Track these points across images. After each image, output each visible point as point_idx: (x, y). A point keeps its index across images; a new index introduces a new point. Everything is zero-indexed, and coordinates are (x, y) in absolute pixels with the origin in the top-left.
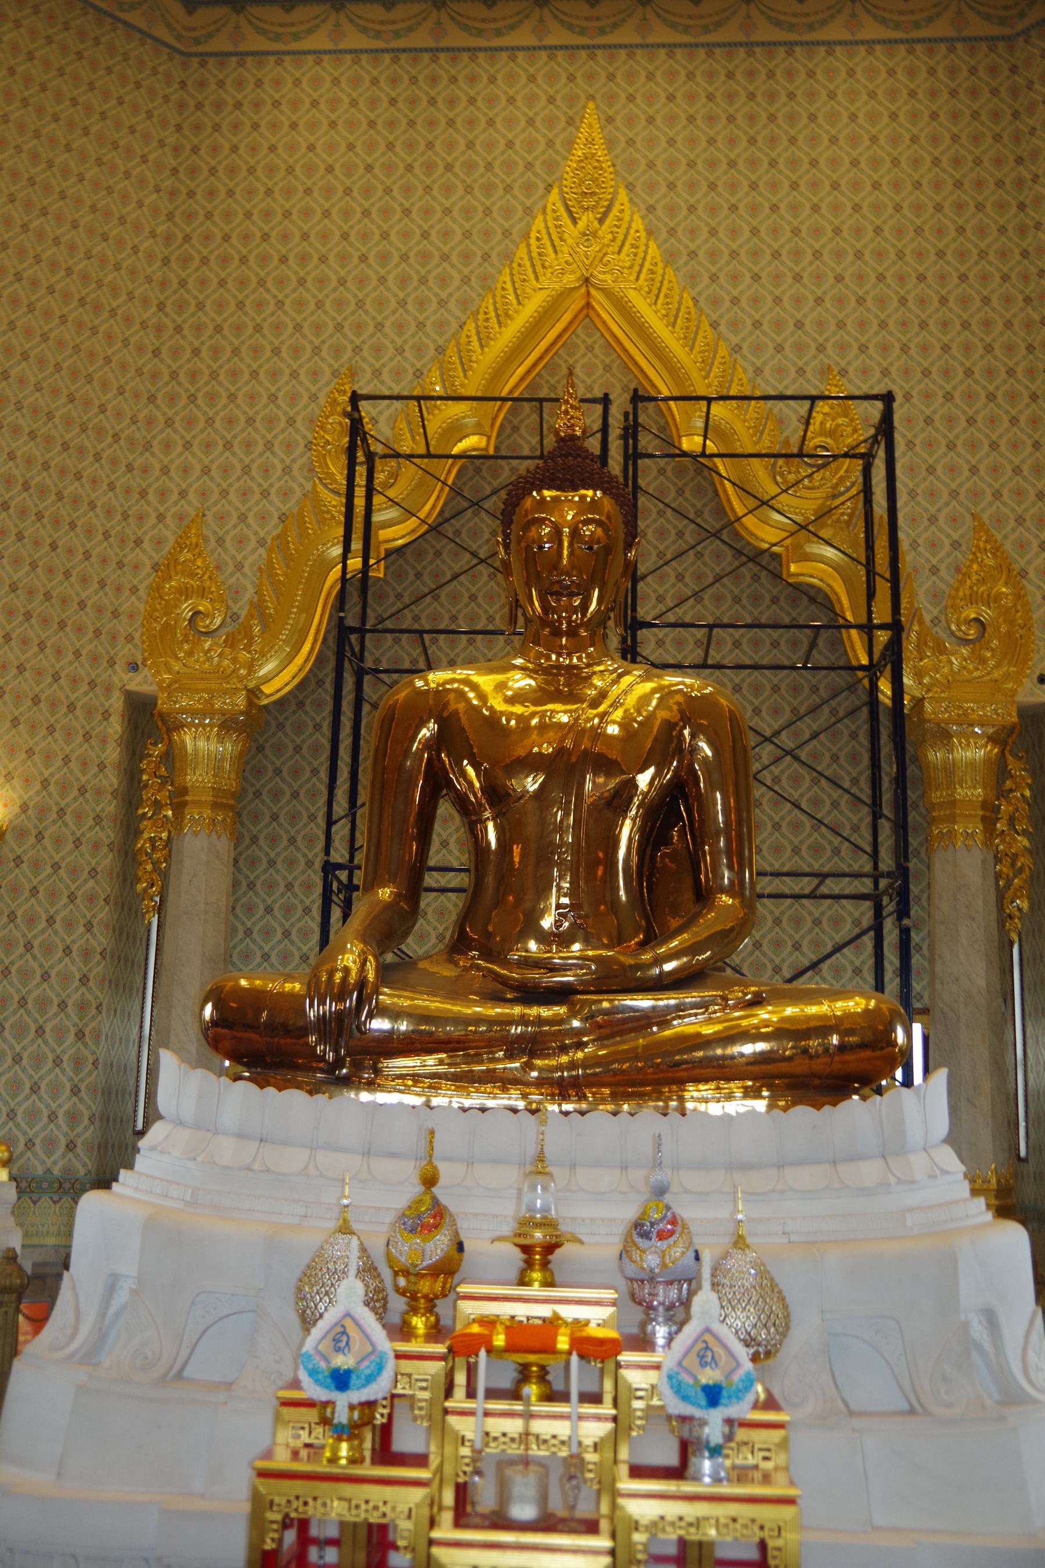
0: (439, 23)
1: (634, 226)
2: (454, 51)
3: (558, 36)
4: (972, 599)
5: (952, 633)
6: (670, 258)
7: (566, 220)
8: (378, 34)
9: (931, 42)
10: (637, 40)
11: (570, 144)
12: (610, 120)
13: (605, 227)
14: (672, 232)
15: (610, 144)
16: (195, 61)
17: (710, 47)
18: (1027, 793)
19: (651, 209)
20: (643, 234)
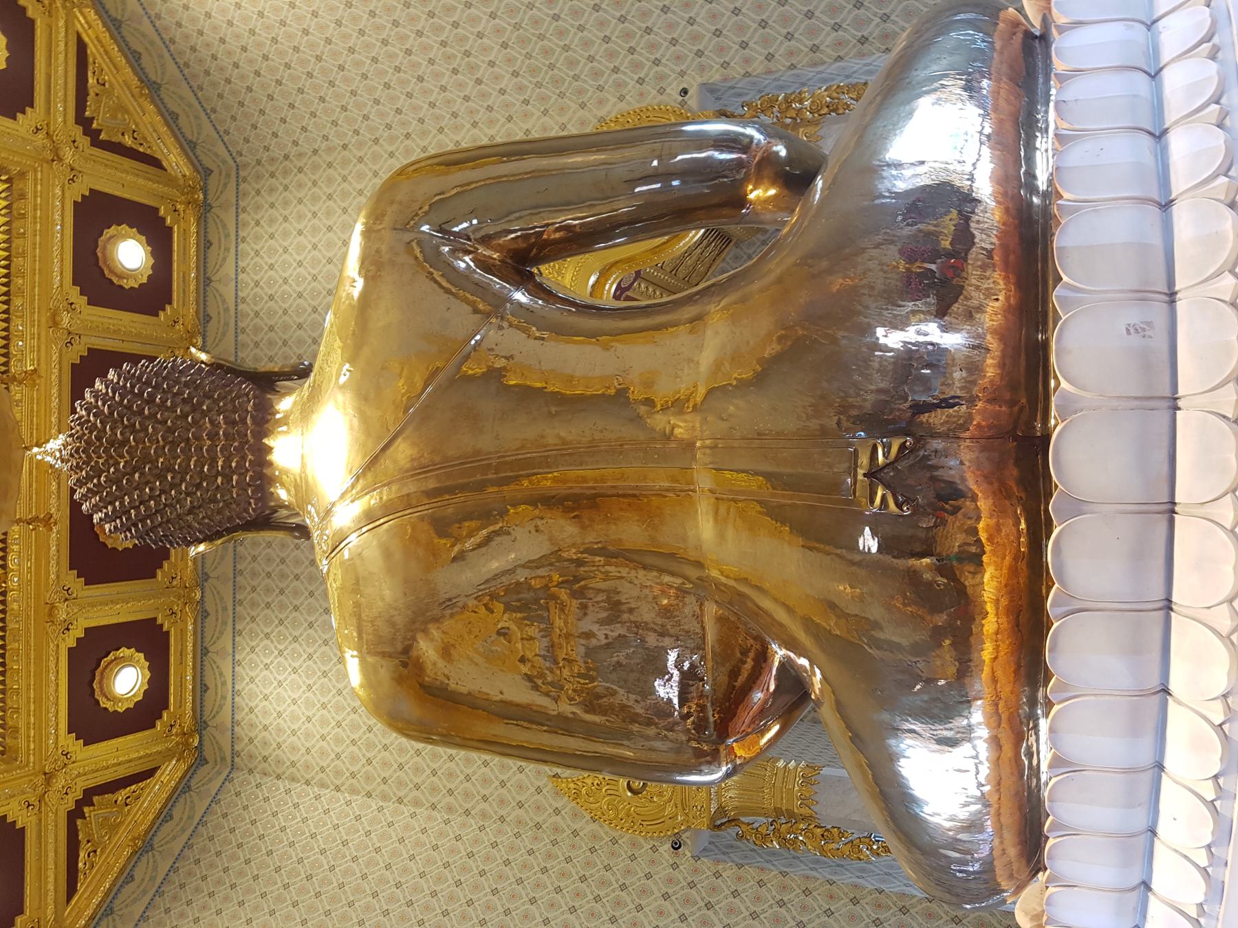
16: (236, 760)
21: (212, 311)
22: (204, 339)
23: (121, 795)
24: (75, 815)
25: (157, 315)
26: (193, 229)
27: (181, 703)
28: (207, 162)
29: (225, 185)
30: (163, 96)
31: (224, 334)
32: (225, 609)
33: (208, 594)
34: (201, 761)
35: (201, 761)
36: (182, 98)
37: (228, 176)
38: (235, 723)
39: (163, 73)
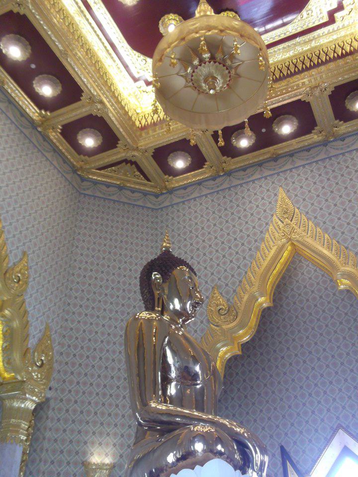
0: (230, 180)
2: (235, 186)
3: (267, 173)
6: (317, 225)
7: (280, 223)
10: (292, 167)
11: (277, 201)
12: (288, 191)
13: (293, 221)
14: (316, 218)
15: (290, 198)
17: (317, 162)
19: (307, 213)
21: (347, 140)
22: (333, 141)
23: (138, 173)
24: (126, 161)
25: (336, 119)
27: (177, 182)
31: (337, 149)
32: (218, 187)
33: (223, 178)
34: (157, 196)
35: (157, 196)
38: (172, 206)
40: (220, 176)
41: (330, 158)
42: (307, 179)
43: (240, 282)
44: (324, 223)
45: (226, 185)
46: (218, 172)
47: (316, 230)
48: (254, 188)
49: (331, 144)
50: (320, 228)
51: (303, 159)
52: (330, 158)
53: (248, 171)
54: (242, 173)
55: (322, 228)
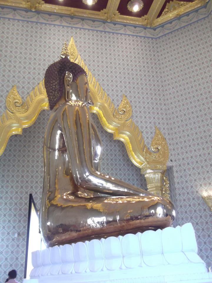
1: (82, 63)
2: (42, 23)
3: (64, 24)
4: (156, 144)
5: (153, 151)
8: (24, 17)
9: (141, 37)
14: (89, 65)
15: (77, 46)
18: (168, 185)
20: (84, 64)
21: (117, 26)
25: (118, 10)
26: (140, 24)
28: (158, 30)
29: (151, 34)
30: (176, 21)
31: (110, 28)
32: (28, 18)
33: (33, 13)
36: (176, 26)
37: (154, 35)
39: (182, 22)
40: (32, 11)
41: (105, 32)
42: (89, 39)
43: (34, 88)
44: (94, 70)
45: (34, 19)
46: (31, 7)
47: (89, 73)
48: (46, 29)
49: (107, 23)
50: (91, 73)
51: (67, 23)
52: (105, 32)
53: (52, 17)
54: (47, 16)
55: (92, 73)
